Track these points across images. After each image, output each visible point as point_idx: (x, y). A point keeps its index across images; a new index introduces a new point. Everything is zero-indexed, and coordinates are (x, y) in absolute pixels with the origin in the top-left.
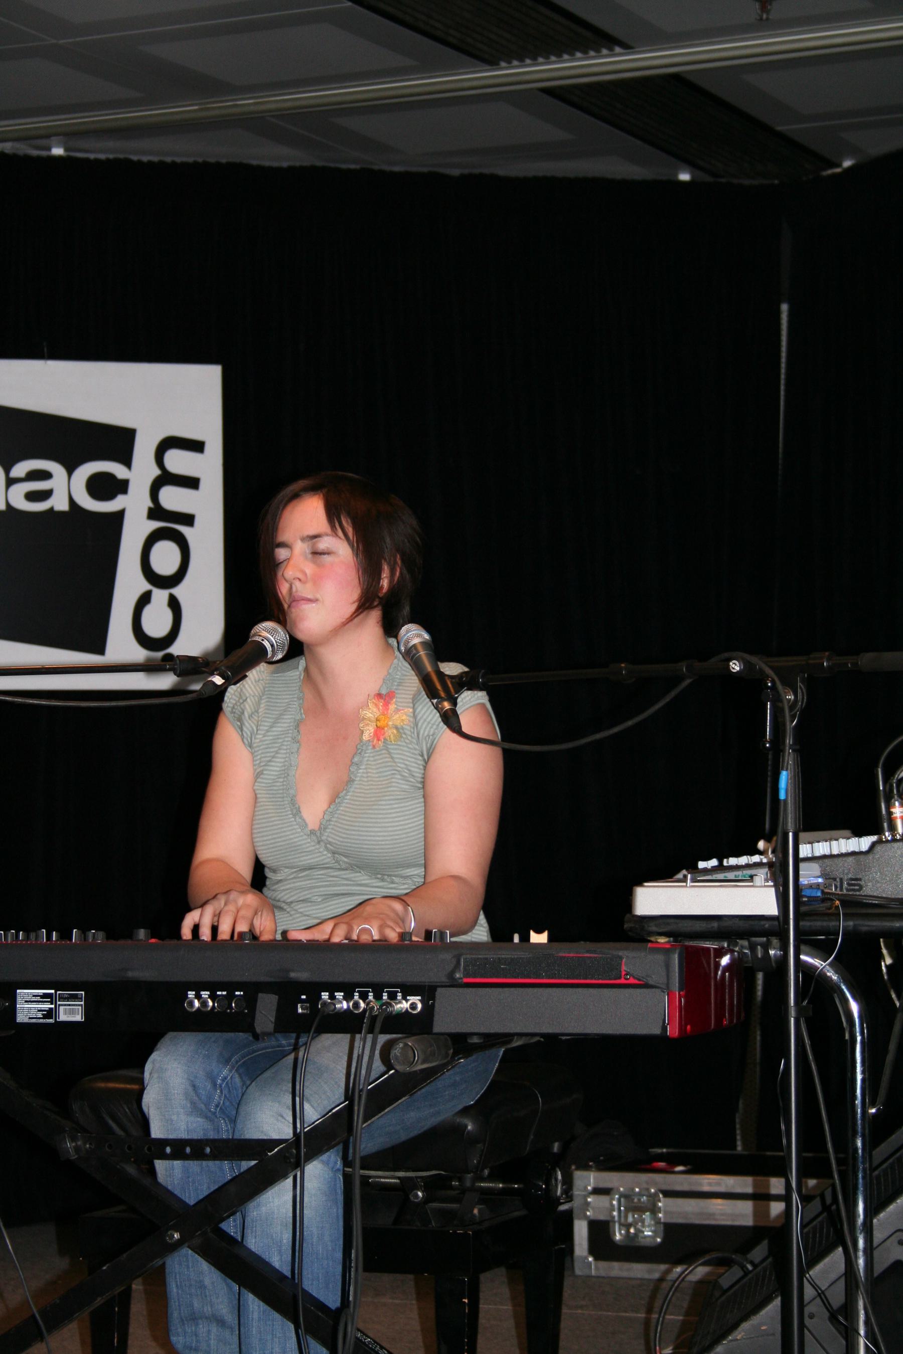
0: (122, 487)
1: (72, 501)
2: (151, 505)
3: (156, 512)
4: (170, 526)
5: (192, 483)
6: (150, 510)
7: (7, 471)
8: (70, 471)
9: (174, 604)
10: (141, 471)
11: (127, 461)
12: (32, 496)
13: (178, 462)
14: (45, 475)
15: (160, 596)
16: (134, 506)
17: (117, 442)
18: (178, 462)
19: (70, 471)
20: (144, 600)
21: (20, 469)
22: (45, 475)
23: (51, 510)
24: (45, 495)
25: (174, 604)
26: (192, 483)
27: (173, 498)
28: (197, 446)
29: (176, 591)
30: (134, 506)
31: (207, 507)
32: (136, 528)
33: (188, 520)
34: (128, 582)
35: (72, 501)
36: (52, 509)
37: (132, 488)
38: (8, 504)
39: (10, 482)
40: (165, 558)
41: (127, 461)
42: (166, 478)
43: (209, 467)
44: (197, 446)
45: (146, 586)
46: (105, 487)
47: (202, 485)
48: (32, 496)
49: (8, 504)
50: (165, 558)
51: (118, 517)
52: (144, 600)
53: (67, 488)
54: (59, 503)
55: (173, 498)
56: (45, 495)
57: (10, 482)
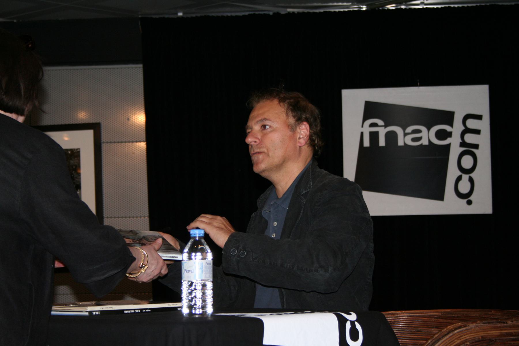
0: (449, 135)
1: (430, 141)
2: (461, 141)
3: (463, 144)
4: (469, 149)
5: (477, 132)
6: (461, 143)
7: (404, 130)
8: (429, 129)
9: (471, 180)
10: (457, 128)
11: (452, 126)
12: (414, 140)
13: (472, 124)
14: (419, 131)
15: (465, 177)
16: (454, 141)
17: (447, 117)
18: (472, 124)
19: (429, 129)
20: (459, 179)
21: (409, 129)
22: (419, 131)
23: (422, 144)
24: (420, 139)
25: (471, 180)
26: (477, 132)
27: (470, 138)
28: (479, 117)
29: (472, 175)
30: (454, 141)
31: (484, 142)
32: (455, 151)
33: (476, 146)
34: (453, 172)
35: (430, 141)
36: (422, 144)
37: (453, 135)
38: (405, 143)
39: (405, 134)
40: (467, 162)
41: (452, 126)
42: (467, 131)
43: (484, 125)
44: (479, 117)
45: (459, 173)
46: (443, 135)
47: (481, 133)
48: (414, 140)
49: (405, 143)
50: (467, 162)
51: (448, 147)
52: (459, 179)
53: (428, 136)
54: (425, 142)
55: (470, 138)
56: (420, 139)
57: (405, 134)
